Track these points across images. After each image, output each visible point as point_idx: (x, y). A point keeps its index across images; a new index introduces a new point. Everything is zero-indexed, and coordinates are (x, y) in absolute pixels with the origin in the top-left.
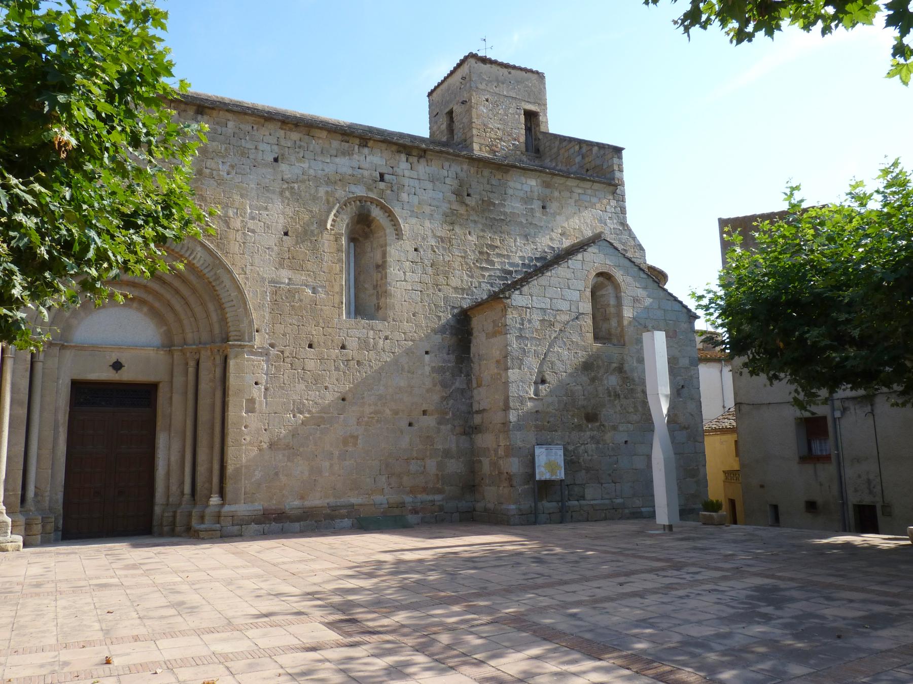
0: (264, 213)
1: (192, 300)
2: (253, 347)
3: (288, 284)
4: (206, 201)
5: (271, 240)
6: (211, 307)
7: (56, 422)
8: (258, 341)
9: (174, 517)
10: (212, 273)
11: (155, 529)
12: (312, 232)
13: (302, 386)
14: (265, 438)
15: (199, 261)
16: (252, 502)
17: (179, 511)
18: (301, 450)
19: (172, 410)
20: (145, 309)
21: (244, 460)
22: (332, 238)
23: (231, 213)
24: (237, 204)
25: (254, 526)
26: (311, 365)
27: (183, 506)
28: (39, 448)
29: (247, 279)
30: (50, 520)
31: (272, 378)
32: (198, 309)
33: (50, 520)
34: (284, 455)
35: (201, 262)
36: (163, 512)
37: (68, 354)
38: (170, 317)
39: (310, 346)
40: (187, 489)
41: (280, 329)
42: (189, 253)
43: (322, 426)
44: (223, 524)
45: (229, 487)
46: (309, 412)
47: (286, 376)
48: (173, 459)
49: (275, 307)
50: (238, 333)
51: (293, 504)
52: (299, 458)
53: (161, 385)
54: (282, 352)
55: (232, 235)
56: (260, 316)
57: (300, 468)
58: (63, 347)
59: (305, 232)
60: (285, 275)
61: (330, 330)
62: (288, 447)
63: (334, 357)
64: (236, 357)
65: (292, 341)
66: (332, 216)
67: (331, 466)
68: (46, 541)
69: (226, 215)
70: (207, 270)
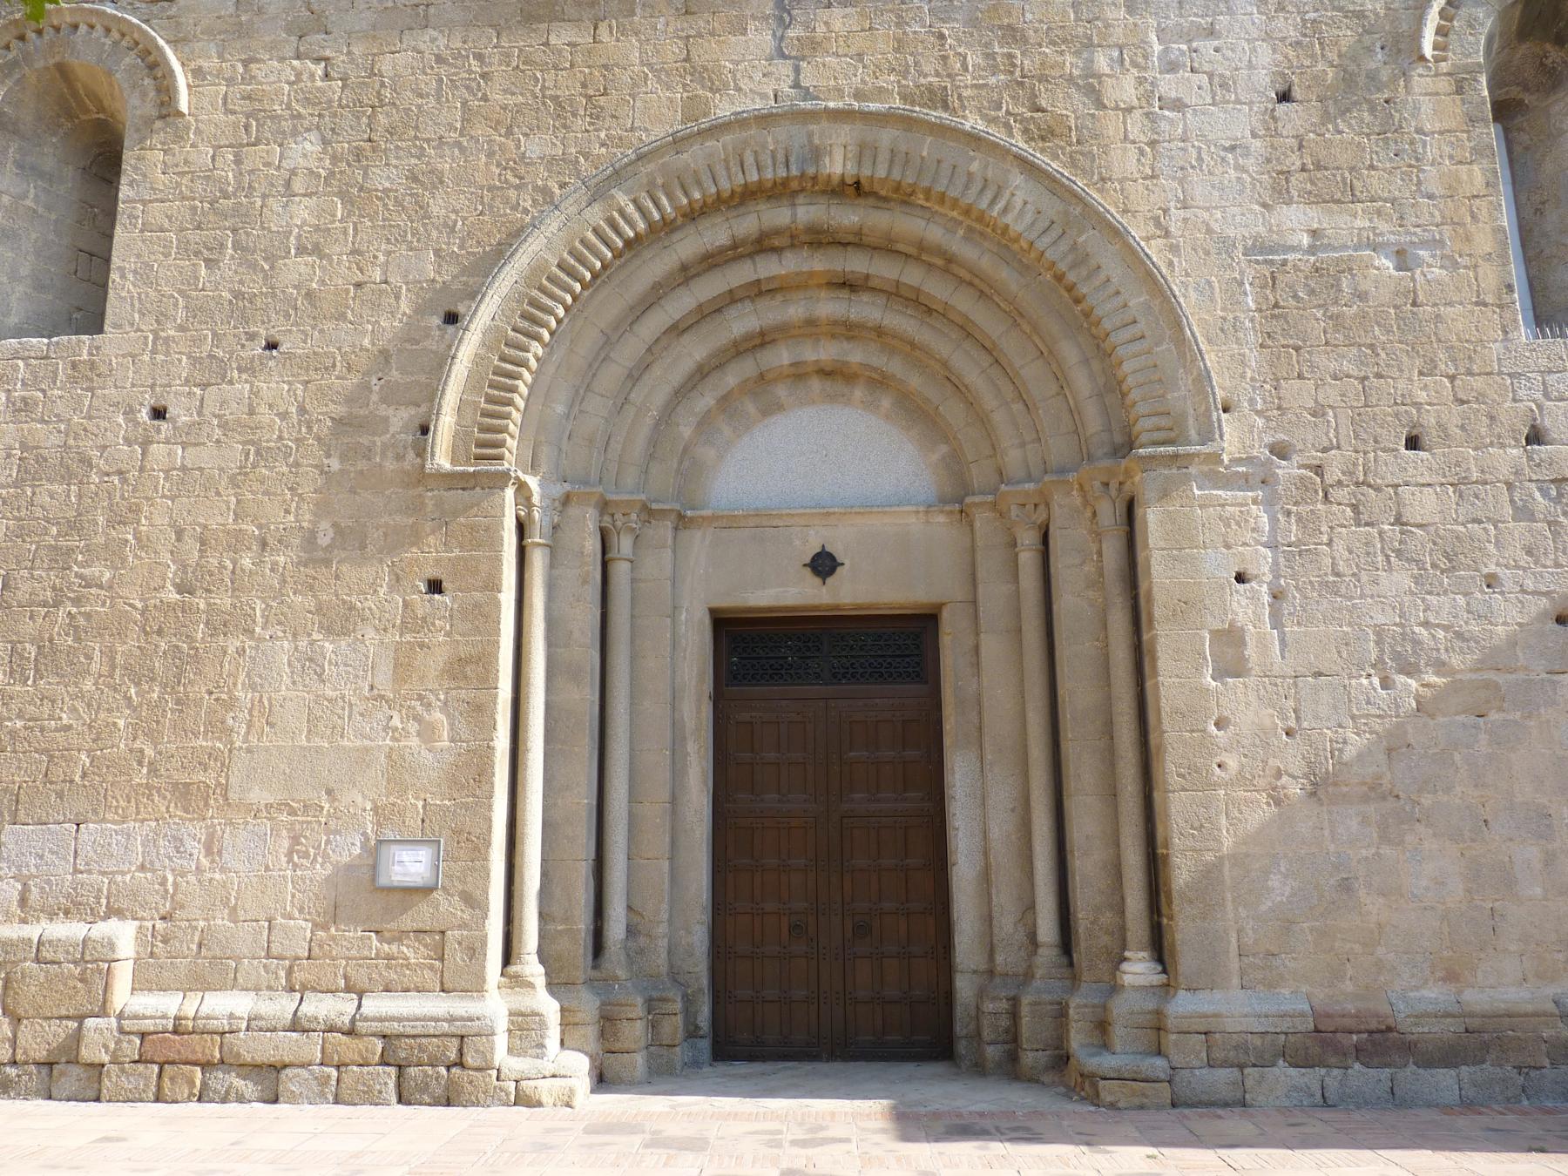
0: (1207, 46)
1: (1011, 345)
2: (1216, 458)
3: (1312, 250)
4: (1025, 40)
5: (1240, 123)
6: (1070, 353)
7: (676, 725)
8: (1234, 439)
9: (1014, 1015)
10: (1064, 246)
11: (961, 1047)
12: (1372, 76)
13: (1401, 579)
14: (1292, 757)
15: (1022, 212)
16: (1271, 986)
17: (1026, 1001)
18: (1427, 800)
19: (983, 684)
20: (886, 403)
21: (1227, 843)
22: (1444, 85)
23: (1102, 62)
24: (1118, 34)
25: (1284, 1074)
26: (1423, 505)
27: (1037, 983)
28: (633, 798)
29: (1174, 249)
30: (669, 1007)
31: (1293, 554)
32: (1031, 371)
33: (669, 1007)
34: (1365, 821)
35: (1028, 218)
36: (981, 994)
37: (699, 543)
38: (953, 412)
39: (1413, 443)
40: (1047, 929)
41: (1300, 394)
42: (989, 195)
43: (1494, 716)
44: (1177, 1059)
45: (1184, 927)
46: (1440, 667)
47: (1340, 547)
48: (995, 832)
49: (1276, 326)
50: (1163, 422)
51: (1418, 997)
52: (1420, 828)
53: (945, 615)
54: (1319, 470)
55: (1112, 125)
56: (1229, 359)
57: (1431, 871)
58: (682, 522)
59: (1348, 80)
60: (1296, 221)
61: (1478, 383)
62: (1375, 791)
63: (1505, 472)
64: (1165, 495)
65: (1346, 430)
66: (1432, 20)
68: (663, 1074)
69: (1090, 72)
70: (1046, 240)
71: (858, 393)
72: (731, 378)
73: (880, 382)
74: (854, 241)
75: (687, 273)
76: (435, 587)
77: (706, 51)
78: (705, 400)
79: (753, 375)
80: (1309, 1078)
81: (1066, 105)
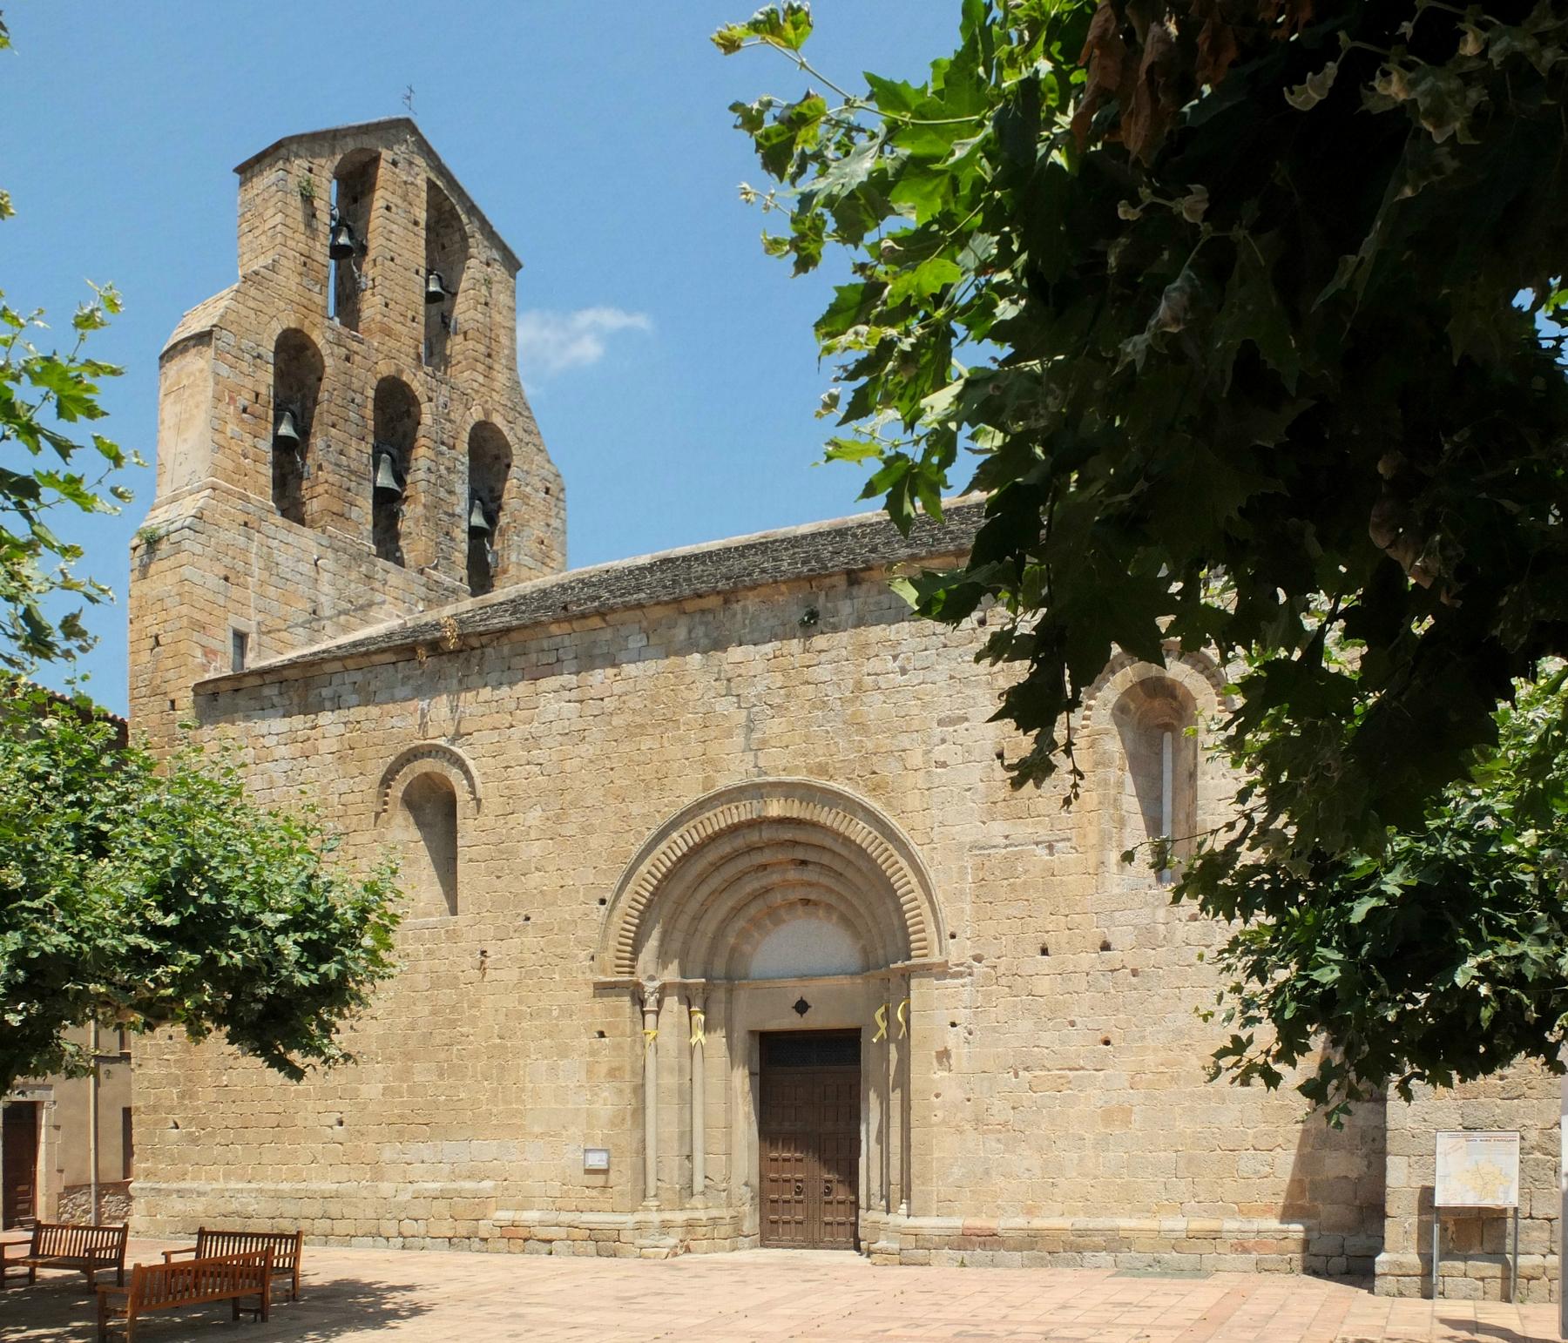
13: (1025, 1025)
26: (1043, 985)
39: (1044, 952)
48: (875, 1149)
60: (998, 828)
63: (1086, 968)
67: (1081, 1159)
71: (821, 913)
72: (752, 910)
73: (829, 908)
74: (795, 843)
75: (716, 867)
76: (602, 1035)
77: (714, 749)
78: (740, 923)
79: (767, 911)
80: (959, 1254)
81: (888, 769)
